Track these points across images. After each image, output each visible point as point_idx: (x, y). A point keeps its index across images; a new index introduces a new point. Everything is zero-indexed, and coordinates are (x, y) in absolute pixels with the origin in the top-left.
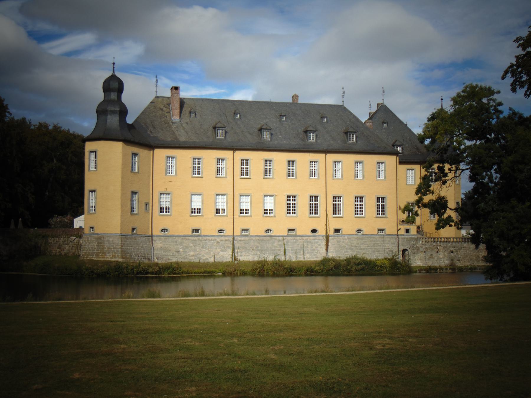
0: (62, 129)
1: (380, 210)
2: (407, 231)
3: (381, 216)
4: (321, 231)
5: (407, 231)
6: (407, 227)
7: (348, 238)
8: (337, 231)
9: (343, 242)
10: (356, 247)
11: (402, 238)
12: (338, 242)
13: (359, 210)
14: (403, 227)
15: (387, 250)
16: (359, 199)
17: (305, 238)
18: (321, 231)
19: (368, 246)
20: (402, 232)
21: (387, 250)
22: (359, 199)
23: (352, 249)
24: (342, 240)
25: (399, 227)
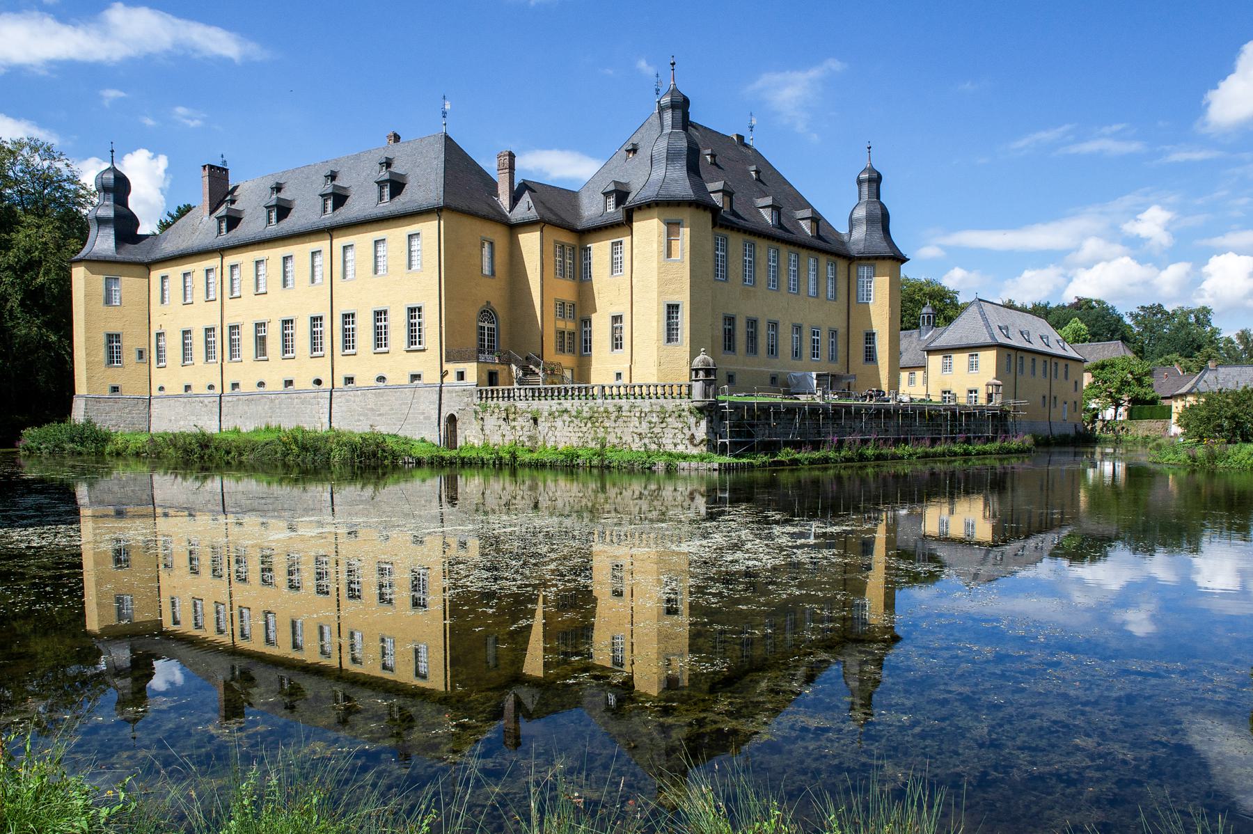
1: (414, 335)
2: (461, 376)
4: (327, 384)
5: (461, 376)
6: (461, 366)
8: (349, 380)
10: (372, 410)
12: (348, 401)
13: (380, 337)
16: (379, 314)
17: (302, 396)
18: (327, 384)
20: (451, 378)
22: (379, 314)
23: (366, 415)
25: (446, 367)
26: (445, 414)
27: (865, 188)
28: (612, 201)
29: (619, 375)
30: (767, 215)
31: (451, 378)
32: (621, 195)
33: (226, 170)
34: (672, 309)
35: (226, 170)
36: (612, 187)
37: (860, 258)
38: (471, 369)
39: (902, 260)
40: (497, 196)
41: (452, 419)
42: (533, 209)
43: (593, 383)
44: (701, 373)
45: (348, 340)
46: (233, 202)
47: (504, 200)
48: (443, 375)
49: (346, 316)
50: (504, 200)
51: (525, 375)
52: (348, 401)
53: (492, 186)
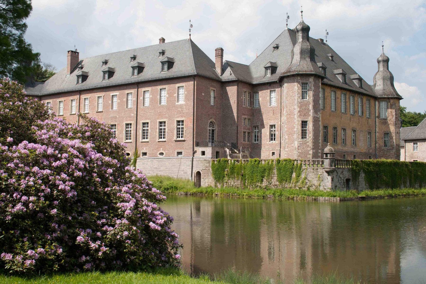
0: (407, 111)
1: (180, 132)
2: (203, 153)
3: (181, 139)
5: (203, 153)
7: (151, 161)
9: (147, 164)
10: (156, 168)
11: (197, 160)
12: (144, 164)
14: (199, 150)
15: (182, 172)
19: (167, 168)
21: (182, 172)
24: (146, 163)
25: (196, 149)
26: (195, 171)
27: (381, 64)
28: (269, 71)
29: (273, 153)
30: (340, 78)
31: (198, 154)
32: (273, 68)
33: (78, 53)
34: (304, 124)
35: (78, 53)
36: (269, 65)
37: (381, 98)
38: (209, 151)
39: (399, 98)
40: (215, 68)
41: (199, 174)
42: (233, 75)
43: (262, 158)
44: (329, 155)
45: (145, 135)
46: (82, 68)
47: (218, 70)
48: (194, 152)
49: (144, 124)
50: (218, 70)
51: (232, 152)
52: (144, 164)
53: (213, 65)
